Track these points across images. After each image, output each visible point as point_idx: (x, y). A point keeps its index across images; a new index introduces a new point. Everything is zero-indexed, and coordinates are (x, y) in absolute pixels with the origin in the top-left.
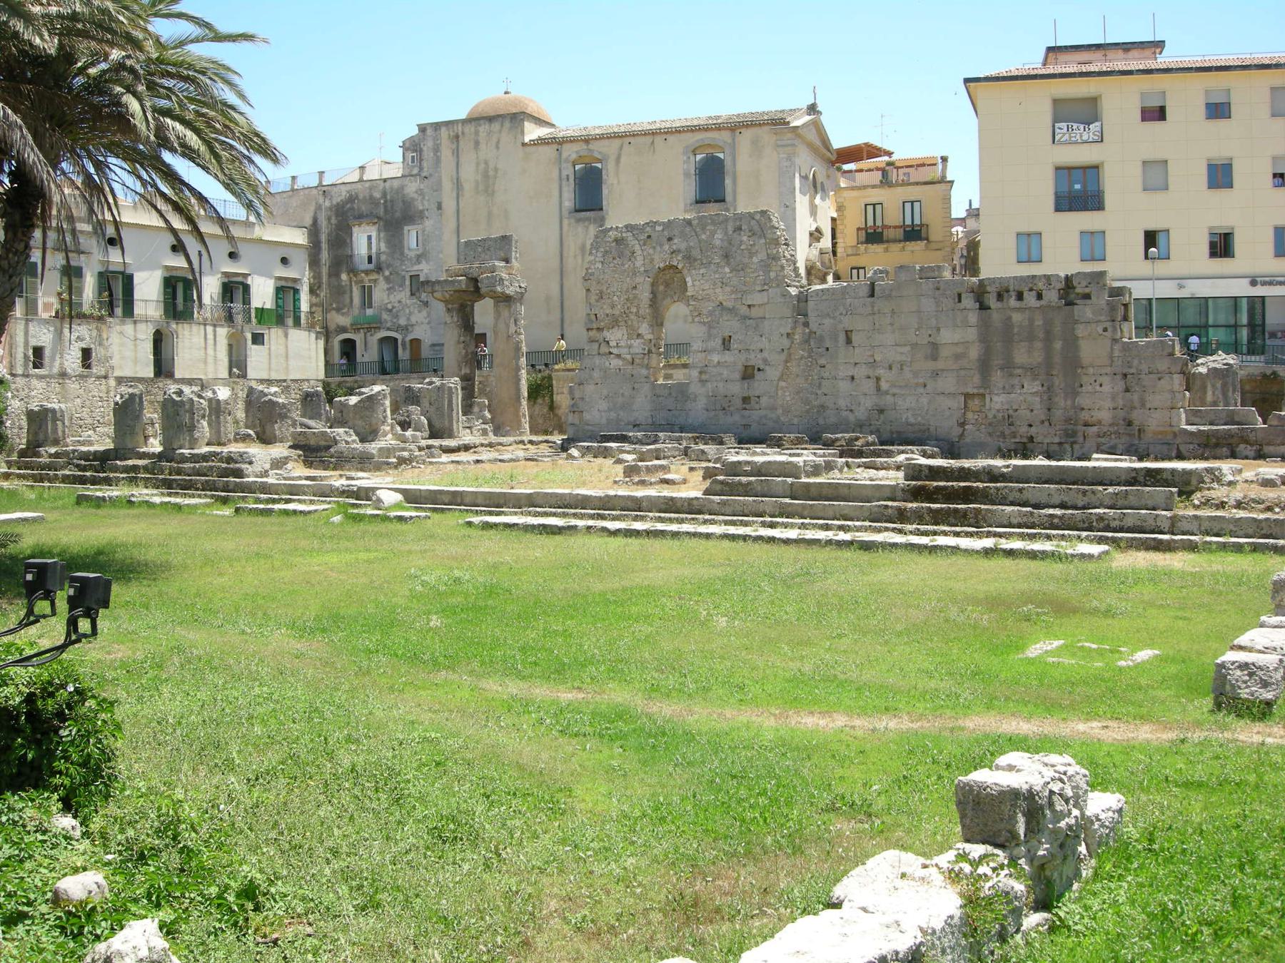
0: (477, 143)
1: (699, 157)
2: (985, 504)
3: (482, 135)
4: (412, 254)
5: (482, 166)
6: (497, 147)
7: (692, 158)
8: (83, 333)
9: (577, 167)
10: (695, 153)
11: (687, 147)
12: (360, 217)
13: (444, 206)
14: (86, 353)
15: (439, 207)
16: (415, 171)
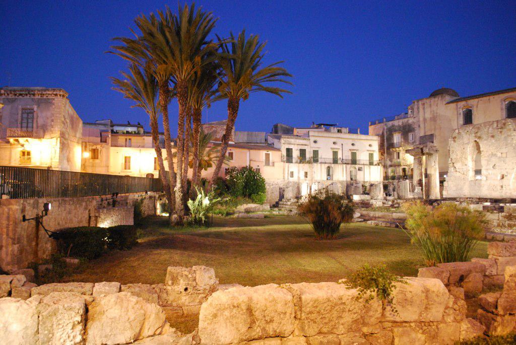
0: (430, 105)
1: (506, 103)
2: (227, 232)
3: (432, 104)
4: (411, 142)
5: (432, 113)
6: (437, 106)
7: (503, 102)
8: (305, 167)
9: (464, 110)
10: (505, 101)
11: (502, 100)
12: (395, 131)
13: (421, 126)
14: (306, 173)
15: (419, 126)
16: (412, 116)
